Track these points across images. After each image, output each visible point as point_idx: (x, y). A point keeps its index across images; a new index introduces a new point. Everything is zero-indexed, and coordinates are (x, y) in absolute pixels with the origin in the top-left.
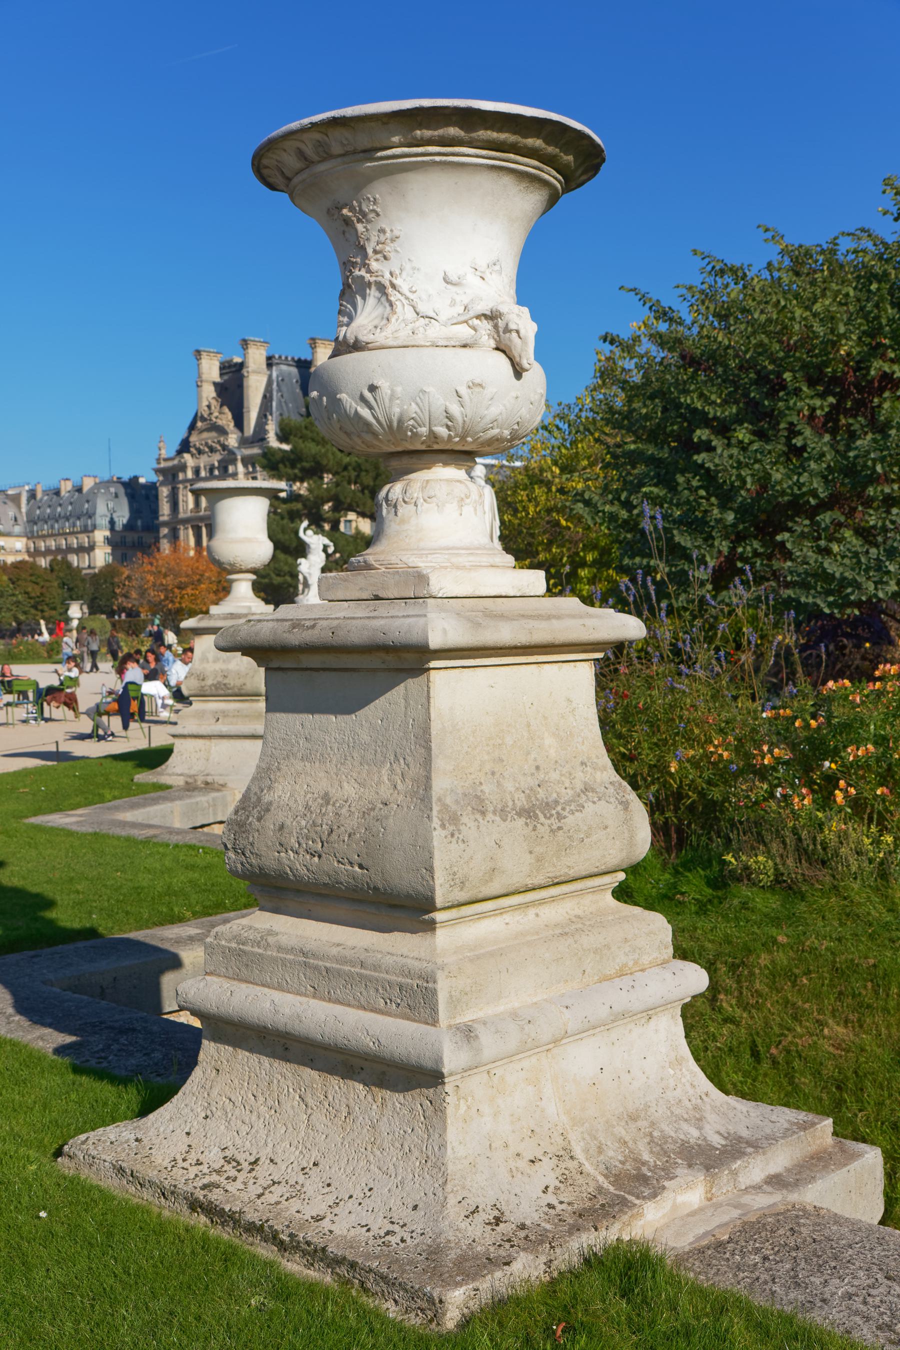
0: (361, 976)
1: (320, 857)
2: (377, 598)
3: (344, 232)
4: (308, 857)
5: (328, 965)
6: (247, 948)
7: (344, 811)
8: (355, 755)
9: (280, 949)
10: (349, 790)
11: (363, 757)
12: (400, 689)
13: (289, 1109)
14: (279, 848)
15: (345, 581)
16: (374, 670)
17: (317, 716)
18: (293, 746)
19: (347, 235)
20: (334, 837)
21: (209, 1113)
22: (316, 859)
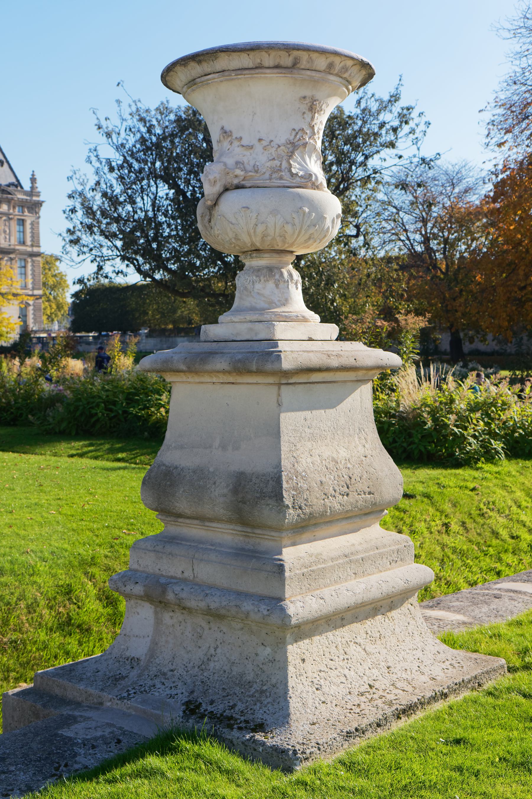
0: (380, 554)
1: (348, 495)
2: (310, 340)
3: (304, 113)
4: (341, 497)
5: (362, 556)
6: (314, 568)
7: (349, 465)
8: (339, 432)
9: (332, 559)
10: (343, 453)
11: (343, 434)
12: (358, 391)
13: (354, 652)
14: (324, 496)
15: (293, 327)
16: (345, 382)
17: (314, 412)
18: (301, 433)
19: (305, 116)
20: (353, 480)
21: (317, 686)
22: (345, 497)
